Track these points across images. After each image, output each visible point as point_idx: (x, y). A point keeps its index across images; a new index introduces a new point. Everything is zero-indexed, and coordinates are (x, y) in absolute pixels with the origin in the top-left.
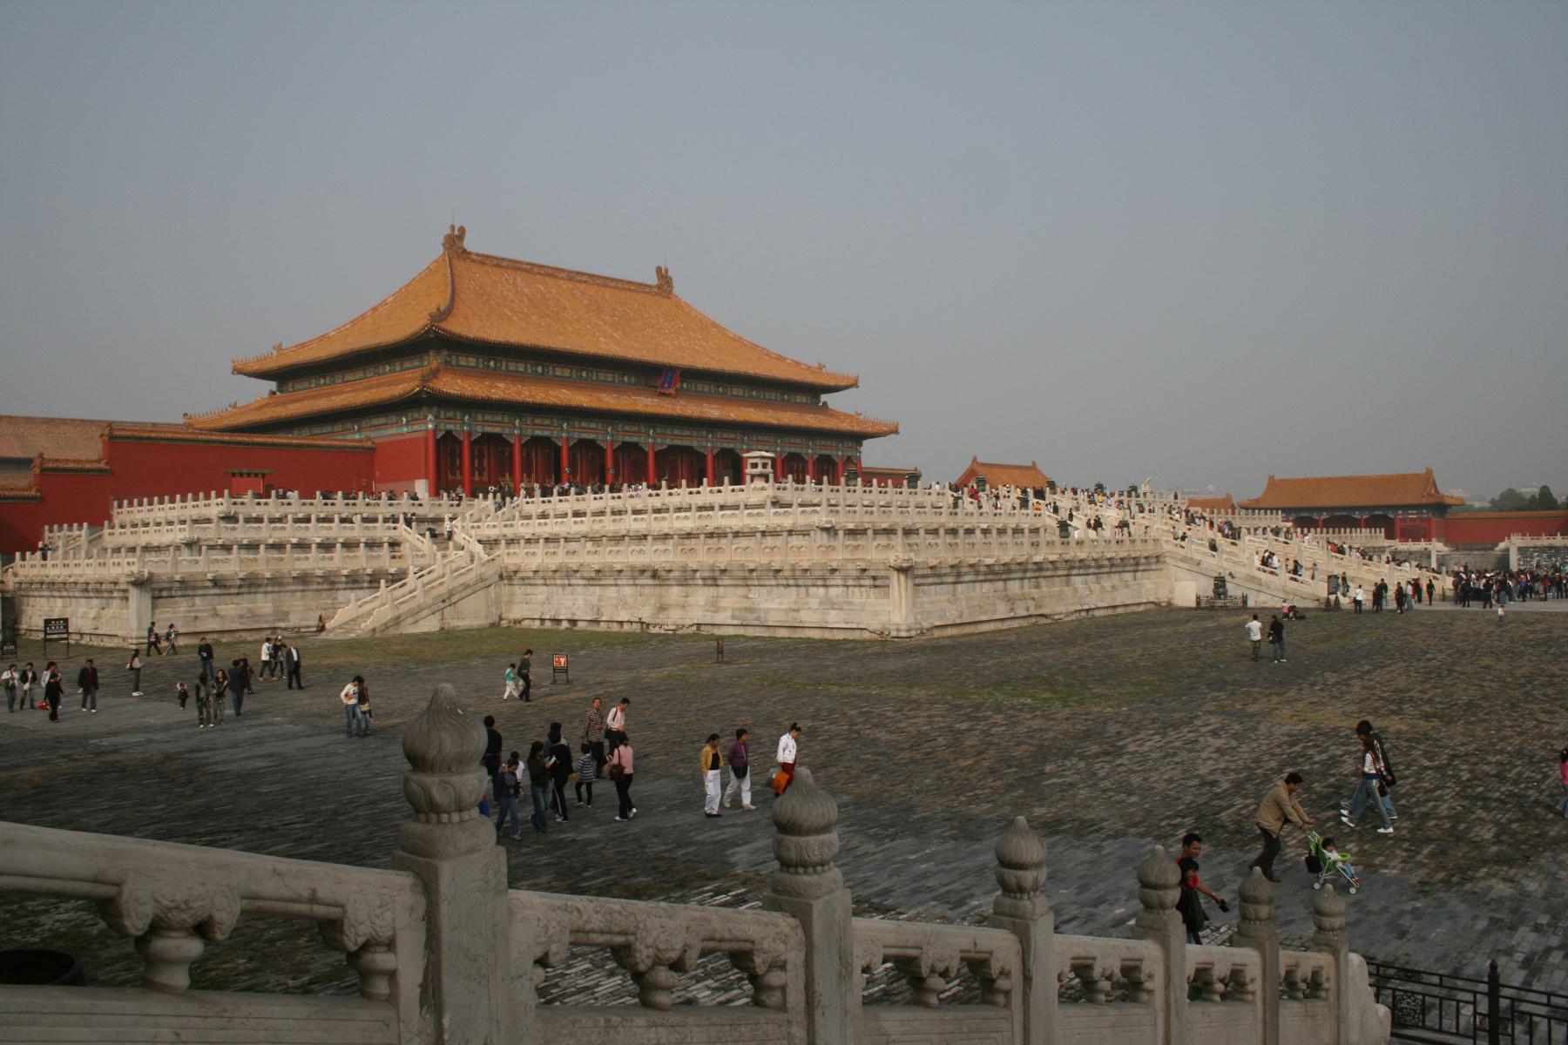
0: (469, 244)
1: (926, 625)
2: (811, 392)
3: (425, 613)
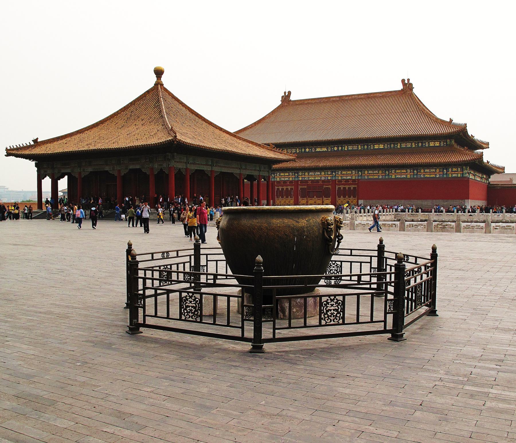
0: (292, 98)
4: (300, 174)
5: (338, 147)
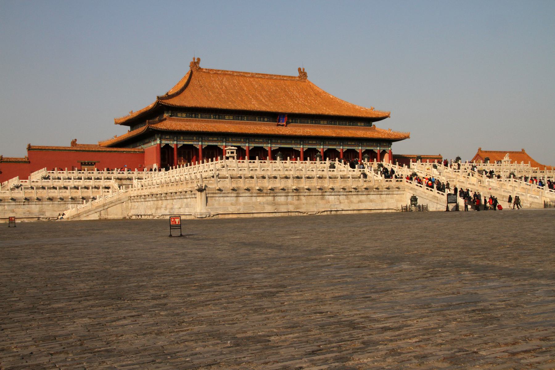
0: (202, 65)
1: (212, 213)
2: (368, 121)
3: (92, 212)
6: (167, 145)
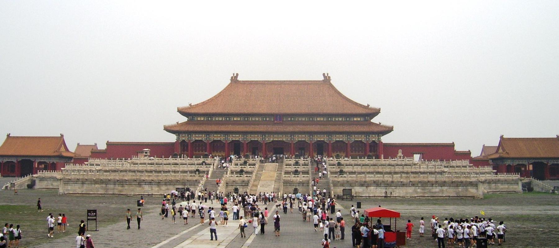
0: (239, 79)
1: (66, 192)
4: (267, 136)
5: (291, 118)
6: (184, 140)
